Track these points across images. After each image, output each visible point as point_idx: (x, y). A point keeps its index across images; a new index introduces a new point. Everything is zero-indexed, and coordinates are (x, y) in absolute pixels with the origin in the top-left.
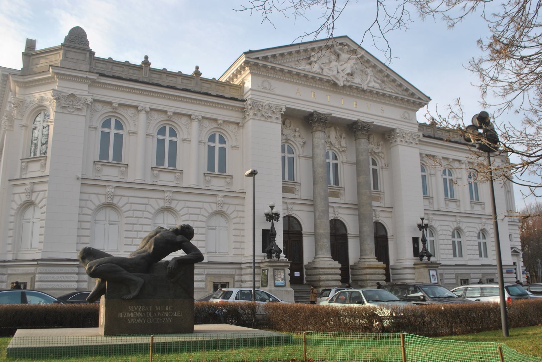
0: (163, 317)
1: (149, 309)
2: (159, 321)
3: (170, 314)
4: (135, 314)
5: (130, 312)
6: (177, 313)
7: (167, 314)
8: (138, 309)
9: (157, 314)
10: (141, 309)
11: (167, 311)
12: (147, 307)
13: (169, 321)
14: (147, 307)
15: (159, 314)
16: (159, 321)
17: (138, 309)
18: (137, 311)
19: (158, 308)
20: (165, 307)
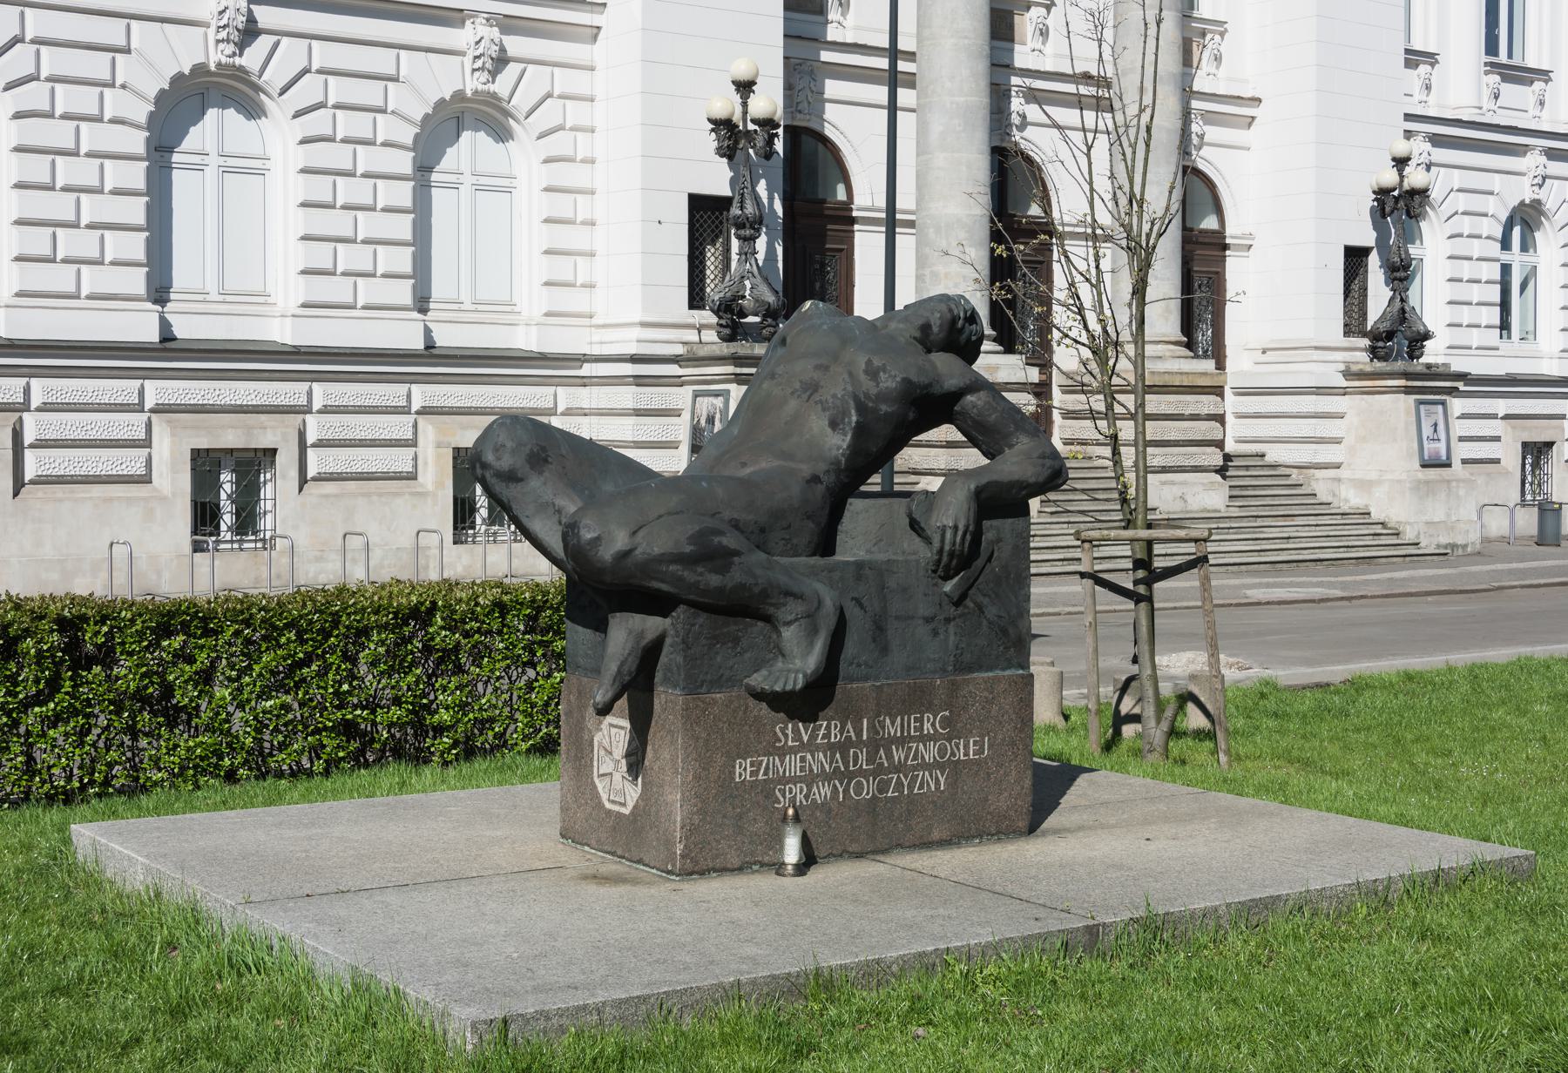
0: (915, 768)
1: (859, 733)
2: (899, 784)
3: (942, 751)
4: (803, 759)
5: (782, 753)
6: (966, 747)
7: (930, 753)
8: (813, 737)
9: (889, 756)
10: (827, 736)
11: (930, 738)
12: (849, 726)
13: (937, 782)
14: (849, 726)
15: (898, 755)
16: (899, 784)
17: (813, 737)
18: (811, 747)
19: (892, 728)
20: (920, 720)
